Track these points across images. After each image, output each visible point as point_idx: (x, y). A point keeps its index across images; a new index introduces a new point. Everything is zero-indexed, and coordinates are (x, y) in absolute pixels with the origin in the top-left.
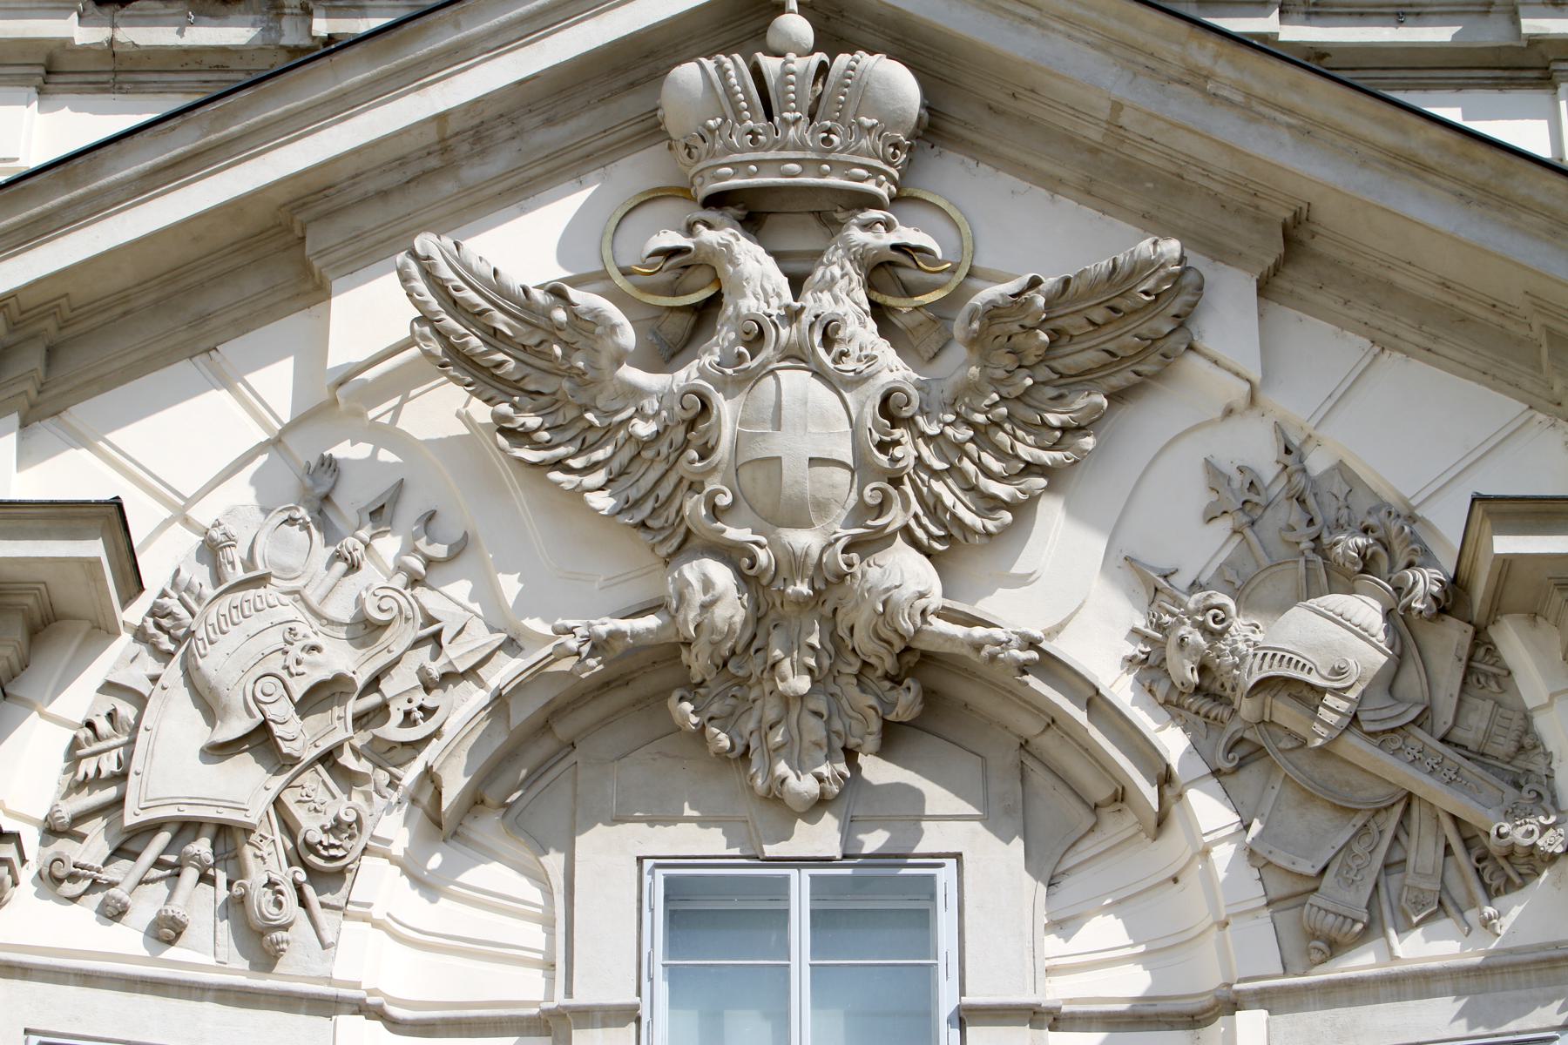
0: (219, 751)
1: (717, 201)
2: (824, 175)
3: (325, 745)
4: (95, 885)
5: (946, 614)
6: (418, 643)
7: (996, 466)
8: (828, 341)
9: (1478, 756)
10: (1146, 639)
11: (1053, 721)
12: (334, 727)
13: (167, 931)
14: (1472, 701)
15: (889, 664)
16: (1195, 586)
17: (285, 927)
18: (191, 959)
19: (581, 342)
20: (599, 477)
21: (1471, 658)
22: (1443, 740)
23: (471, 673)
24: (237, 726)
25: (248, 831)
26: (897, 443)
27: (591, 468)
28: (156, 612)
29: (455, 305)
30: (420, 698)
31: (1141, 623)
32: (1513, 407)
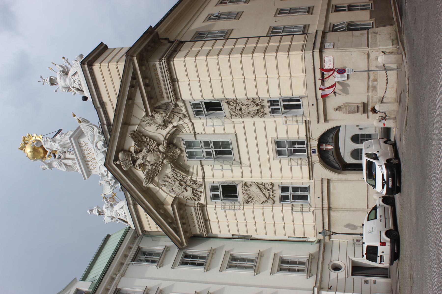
0: (187, 190)
1: (134, 165)
2: (130, 159)
7: (150, 143)
8: (144, 157)
12: (182, 183)
13: (201, 192)
14: (162, 108)
19: (148, 173)
20: (158, 169)
24: (184, 190)
27: (158, 169)
29: (148, 182)
31: (161, 129)
32: (135, 106)
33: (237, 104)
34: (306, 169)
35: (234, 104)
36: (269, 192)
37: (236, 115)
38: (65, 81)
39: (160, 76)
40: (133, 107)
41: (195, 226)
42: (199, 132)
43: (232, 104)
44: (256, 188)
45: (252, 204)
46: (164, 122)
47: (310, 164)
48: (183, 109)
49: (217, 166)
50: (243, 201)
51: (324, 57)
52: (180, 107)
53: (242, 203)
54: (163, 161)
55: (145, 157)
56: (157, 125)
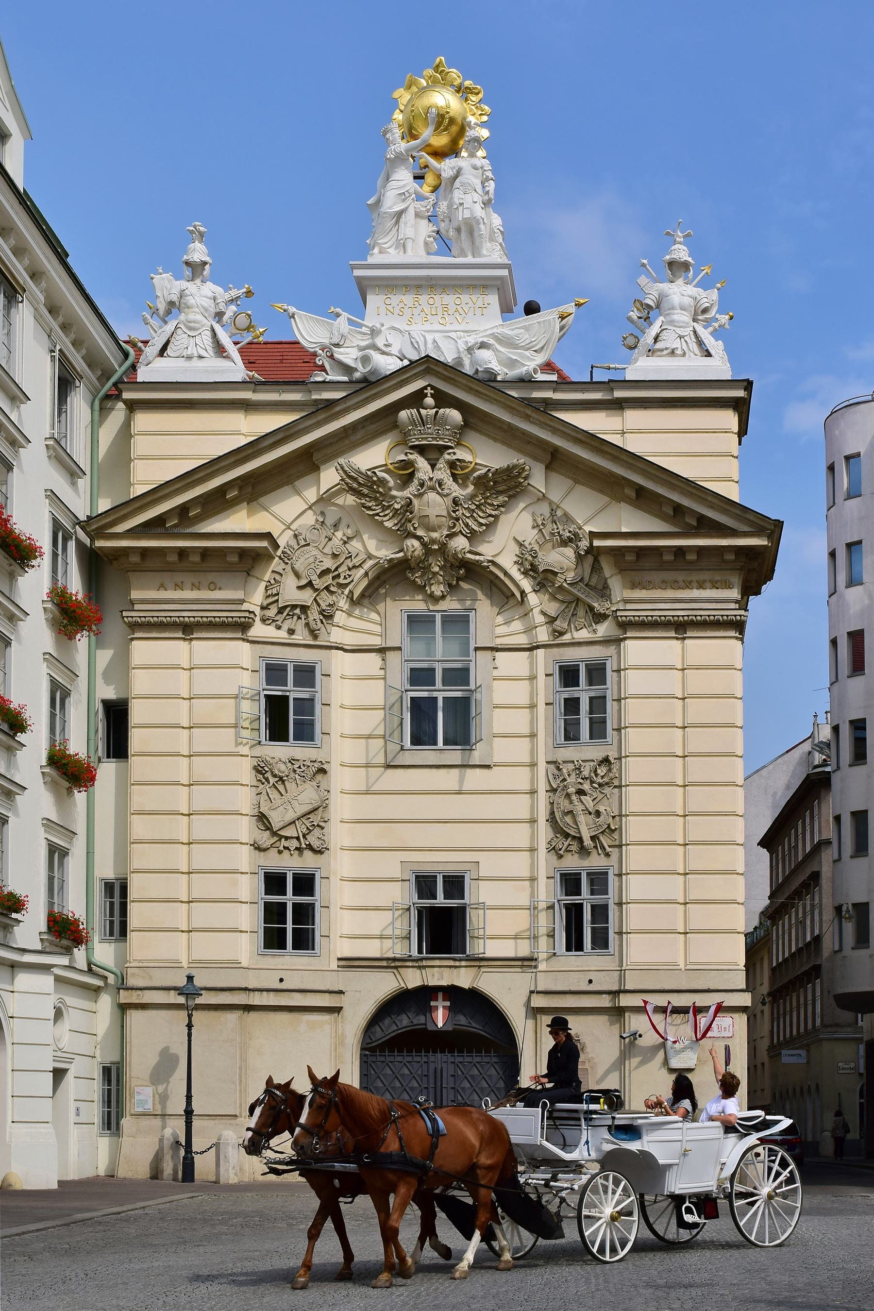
0: (300, 588)
3: (326, 585)
4: (274, 621)
5: (470, 552)
6: (346, 558)
7: (481, 514)
9: (593, 588)
10: (519, 556)
11: (497, 577)
12: (328, 580)
13: (291, 632)
15: (457, 564)
16: (530, 544)
17: (319, 630)
18: (298, 638)
20: (388, 518)
21: (593, 564)
22: (586, 585)
23: (360, 565)
24: (304, 582)
25: (309, 607)
26: (458, 510)
27: (385, 516)
28: (283, 552)
30: (348, 572)
33: (600, 785)
34: (372, 949)
35: (599, 777)
36: (298, 838)
37: (561, 778)
38: (682, 308)
39: (696, 593)
40: (602, 492)
41: (162, 587)
42: (498, 662)
43: (602, 771)
44: (313, 801)
45: (255, 783)
46: (546, 571)
47: (393, 964)
48: (583, 634)
49: (375, 693)
50: (268, 759)
51: (733, 1015)
52: (595, 627)
53: (258, 751)
54: (419, 538)
55: (438, 489)
56: (536, 548)
